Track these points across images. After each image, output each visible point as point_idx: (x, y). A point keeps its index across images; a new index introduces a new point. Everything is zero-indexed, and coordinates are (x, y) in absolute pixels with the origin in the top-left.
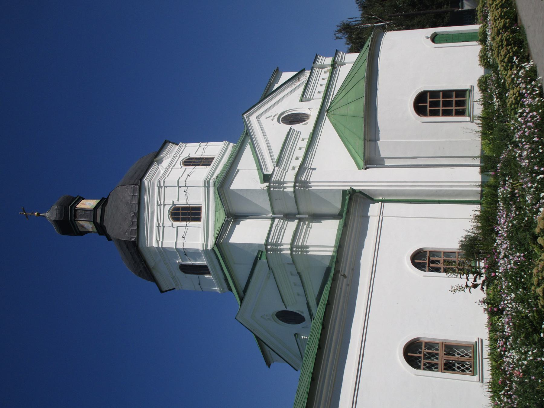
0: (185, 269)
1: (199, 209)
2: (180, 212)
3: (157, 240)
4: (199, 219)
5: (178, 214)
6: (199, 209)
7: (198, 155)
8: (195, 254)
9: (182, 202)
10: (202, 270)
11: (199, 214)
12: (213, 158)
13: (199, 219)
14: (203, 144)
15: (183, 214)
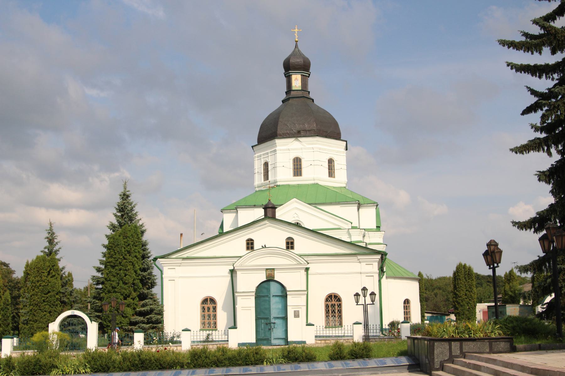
0: (266, 164)
1: (301, 175)
2: (299, 163)
3: (281, 150)
4: (295, 175)
5: (297, 162)
6: (301, 175)
7: (337, 166)
8: (275, 174)
9: (304, 164)
10: (266, 177)
11: (298, 175)
12: (334, 177)
13: (295, 175)
14: (345, 167)
15: (297, 165)
